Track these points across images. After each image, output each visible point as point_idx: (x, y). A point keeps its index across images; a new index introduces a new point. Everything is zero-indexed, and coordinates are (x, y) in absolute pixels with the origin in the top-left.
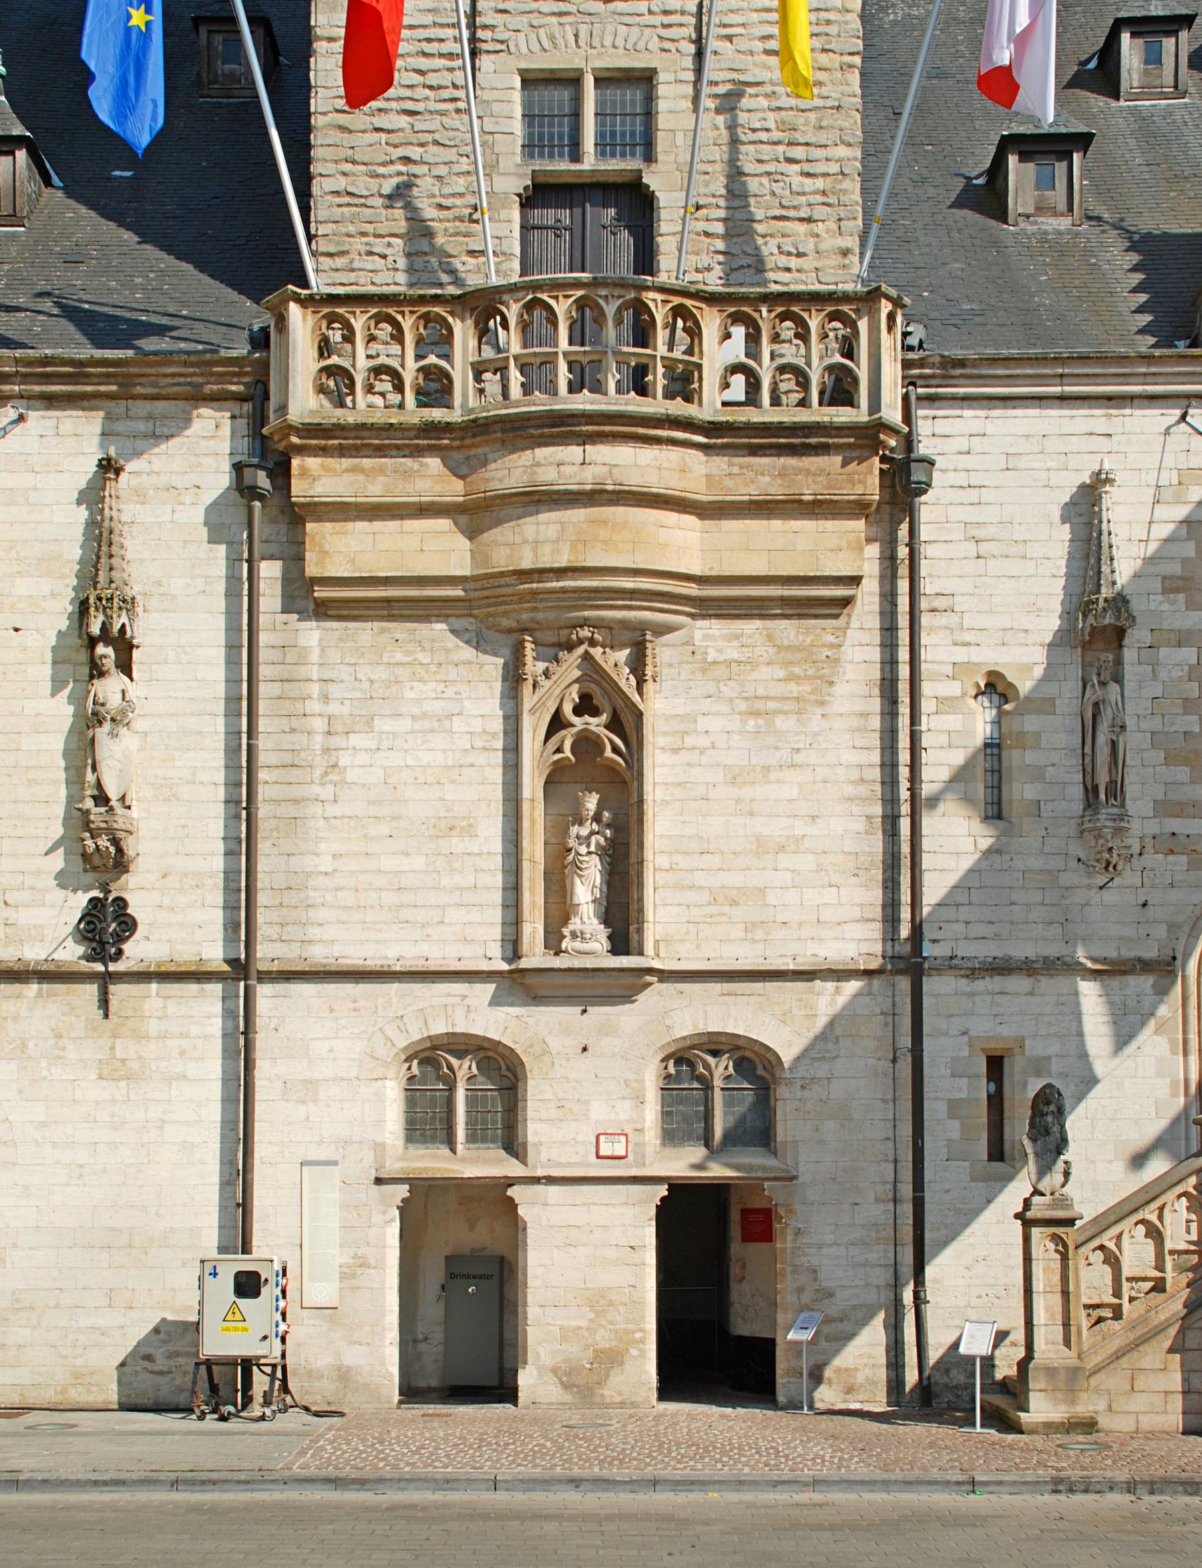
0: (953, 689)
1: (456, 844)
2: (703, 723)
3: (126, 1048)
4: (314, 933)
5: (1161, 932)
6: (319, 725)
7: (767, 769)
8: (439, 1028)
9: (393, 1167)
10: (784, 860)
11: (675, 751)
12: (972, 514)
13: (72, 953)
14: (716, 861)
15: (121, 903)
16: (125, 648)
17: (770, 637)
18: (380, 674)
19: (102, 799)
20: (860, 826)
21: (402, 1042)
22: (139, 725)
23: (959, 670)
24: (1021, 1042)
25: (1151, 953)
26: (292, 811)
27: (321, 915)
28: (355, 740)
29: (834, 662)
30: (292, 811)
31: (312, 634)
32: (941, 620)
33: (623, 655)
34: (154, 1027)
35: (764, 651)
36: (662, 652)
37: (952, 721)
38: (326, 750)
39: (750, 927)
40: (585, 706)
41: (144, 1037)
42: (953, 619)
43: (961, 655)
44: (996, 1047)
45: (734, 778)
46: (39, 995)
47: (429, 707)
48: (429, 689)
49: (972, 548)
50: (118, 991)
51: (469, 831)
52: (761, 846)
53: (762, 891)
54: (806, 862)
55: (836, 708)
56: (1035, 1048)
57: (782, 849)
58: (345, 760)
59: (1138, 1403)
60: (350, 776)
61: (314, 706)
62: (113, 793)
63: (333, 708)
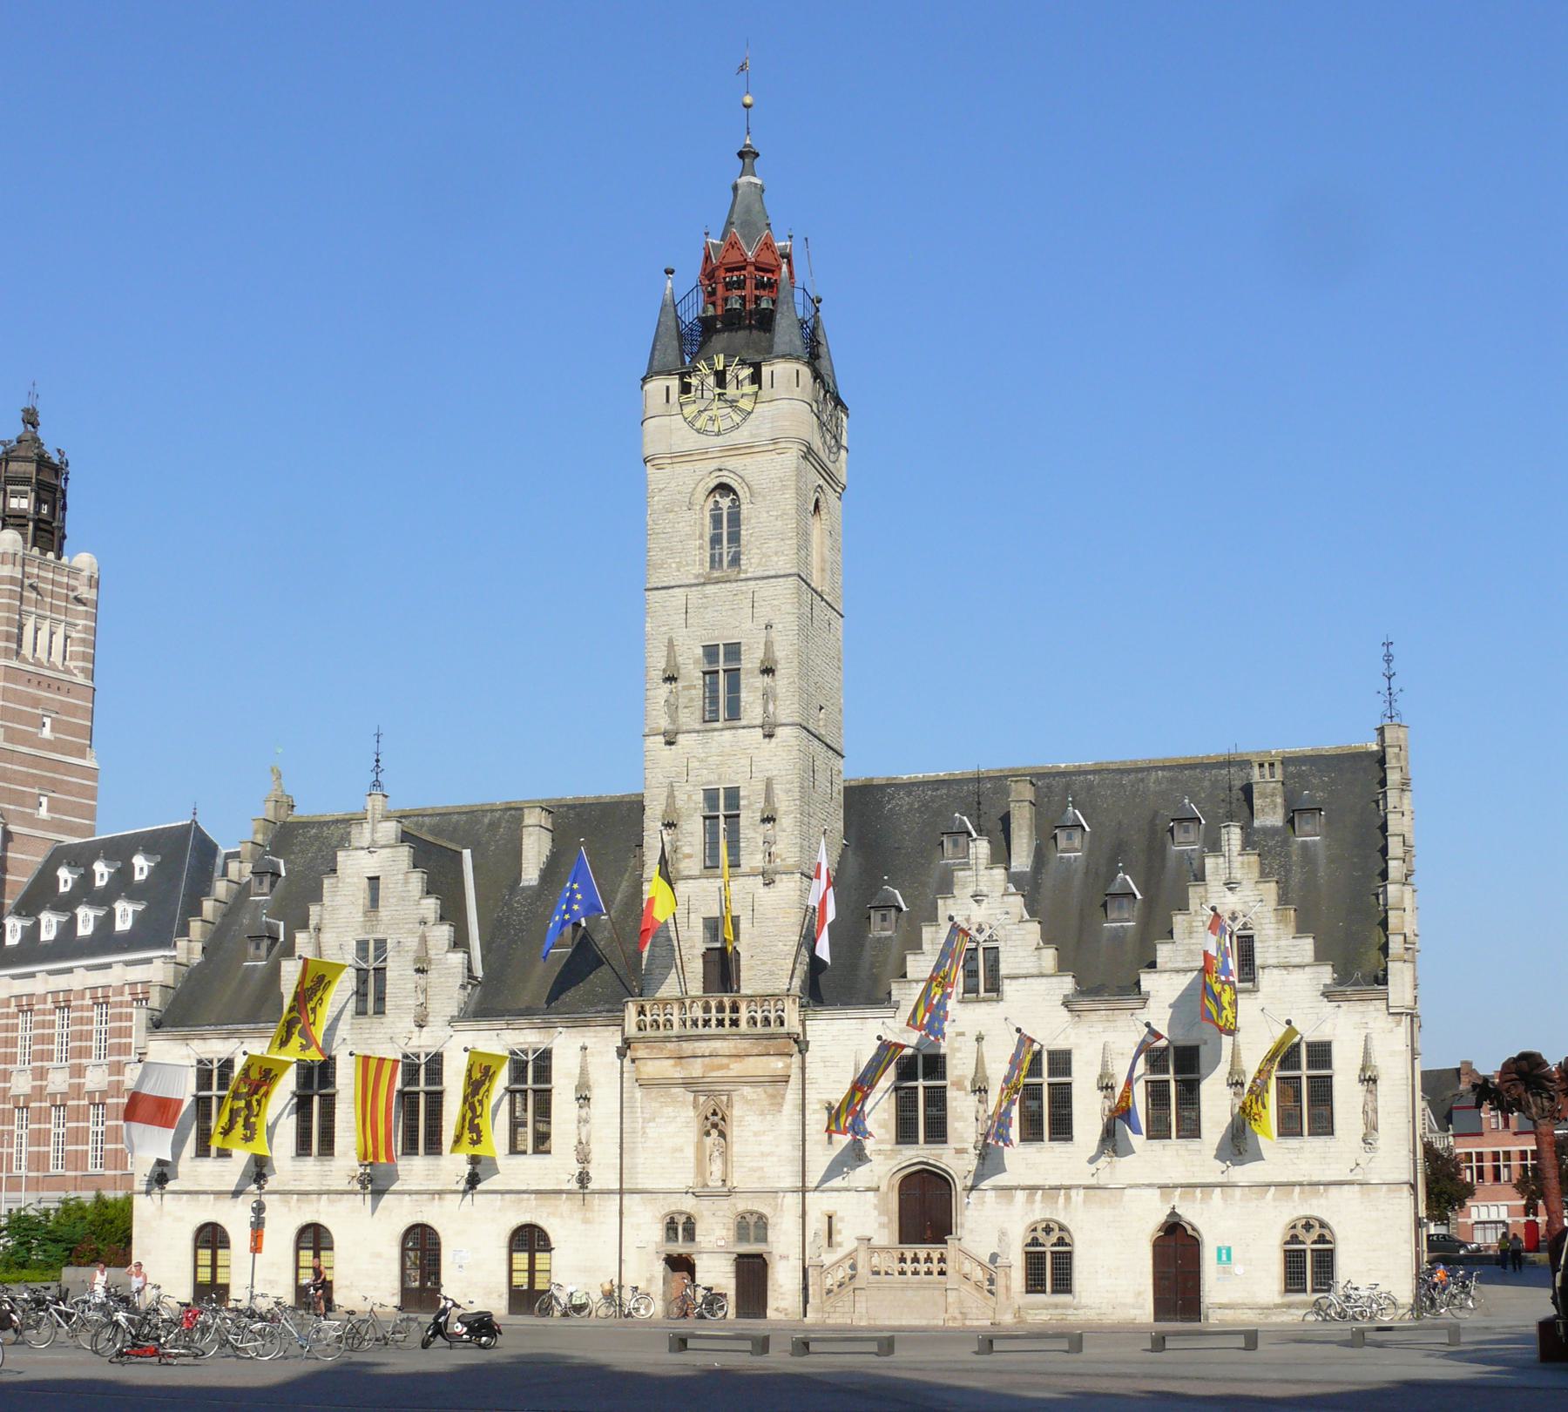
0: (818, 1107)
1: (677, 1155)
2: (747, 1118)
3: (589, 1215)
4: (639, 1181)
5: (876, 1179)
6: (640, 1120)
7: (764, 1132)
8: (673, 1209)
9: (663, 1249)
10: (769, 1158)
11: (739, 1126)
12: (823, 1054)
13: (575, 1186)
14: (749, 1159)
15: (588, 1173)
16: (587, 1099)
17: (765, 1092)
18: (658, 1105)
19: (580, 1143)
20: (790, 1148)
21: (663, 1213)
22: (592, 1121)
23: (820, 1101)
24: (836, 1212)
25: (874, 1185)
26: (632, 1145)
27: (640, 1176)
28: (651, 1124)
29: (783, 1097)
30: (632, 1145)
31: (638, 1093)
32: (814, 1086)
33: (724, 1098)
34: (596, 1208)
35: (764, 1096)
36: (735, 1097)
37: (817, 1116)
38: (643, 1128)
39: (759, 1178)
40: (715, 1113)
41: (592, 1211)
42: (817, 1086)
43: (819, 1096)
44: (830, 1213)
45: (756, 1134)
46: (567, 1198)
47: (672, 1114)
48: (670, 1109)
49: (822, 1064)
50: (587, 1197)
51: (681, 1150)
52: (763, 1154)
53: (762, 1168)
54: (775, 1159)
55: (784, 1113)
56: (839, 1214)
57: (768, 1155)
58: (647, 1131)
59: (837, 1315)
60: (650, 1135)
61: (639, 1115)
62: (584, 1142)
63: (645, 1115)
